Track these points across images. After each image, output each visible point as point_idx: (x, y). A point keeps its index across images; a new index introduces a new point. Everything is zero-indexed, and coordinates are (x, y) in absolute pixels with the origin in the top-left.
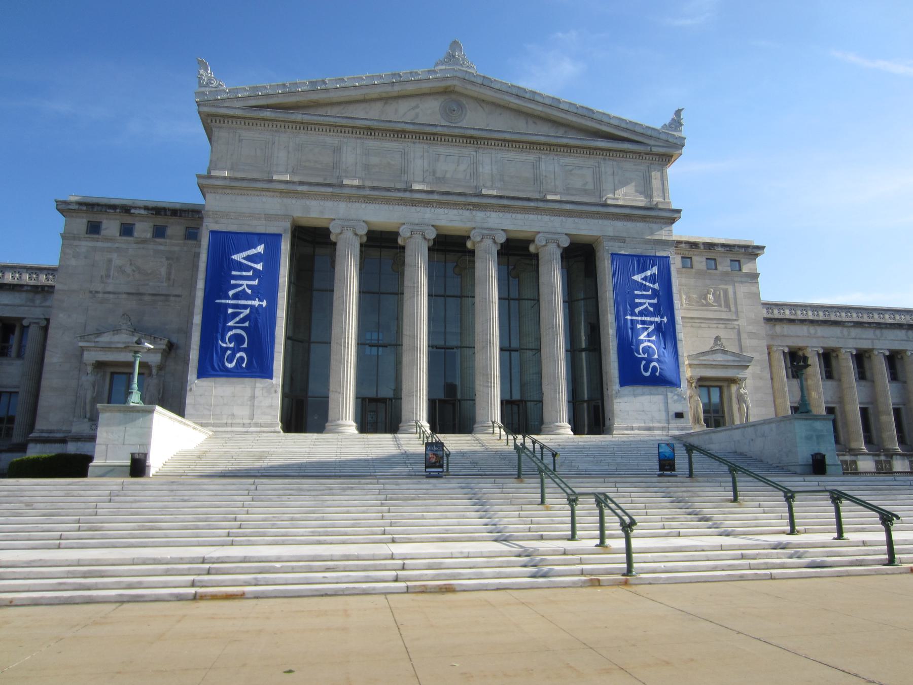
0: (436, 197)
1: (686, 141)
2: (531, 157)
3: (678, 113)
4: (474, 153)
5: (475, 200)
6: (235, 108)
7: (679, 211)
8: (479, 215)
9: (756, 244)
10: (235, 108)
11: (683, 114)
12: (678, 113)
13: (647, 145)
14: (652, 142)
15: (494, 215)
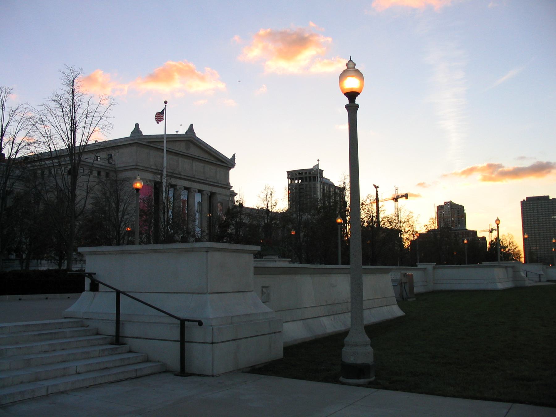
0: (186, 177)
1: (236, 164)
2: (202, 165)
3: (234, 155)
4: (192, 162)
5: (193, 179)
6: (144, 142)
7: (232, 187)
8: (193, 183)
9: (235, 192)
10: (144, 142)
11: (236, 155)
12: (234, 155)
13: (228, 164)
14: (229, 164)
15: (195, 184)
